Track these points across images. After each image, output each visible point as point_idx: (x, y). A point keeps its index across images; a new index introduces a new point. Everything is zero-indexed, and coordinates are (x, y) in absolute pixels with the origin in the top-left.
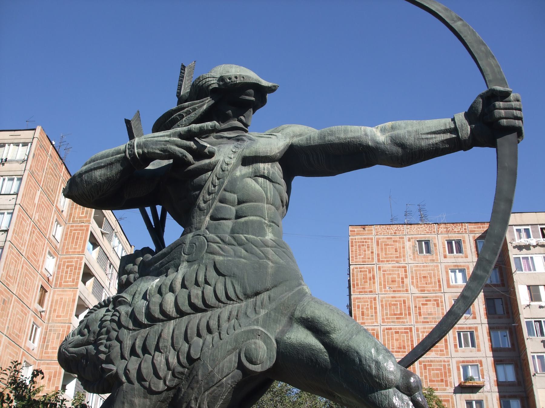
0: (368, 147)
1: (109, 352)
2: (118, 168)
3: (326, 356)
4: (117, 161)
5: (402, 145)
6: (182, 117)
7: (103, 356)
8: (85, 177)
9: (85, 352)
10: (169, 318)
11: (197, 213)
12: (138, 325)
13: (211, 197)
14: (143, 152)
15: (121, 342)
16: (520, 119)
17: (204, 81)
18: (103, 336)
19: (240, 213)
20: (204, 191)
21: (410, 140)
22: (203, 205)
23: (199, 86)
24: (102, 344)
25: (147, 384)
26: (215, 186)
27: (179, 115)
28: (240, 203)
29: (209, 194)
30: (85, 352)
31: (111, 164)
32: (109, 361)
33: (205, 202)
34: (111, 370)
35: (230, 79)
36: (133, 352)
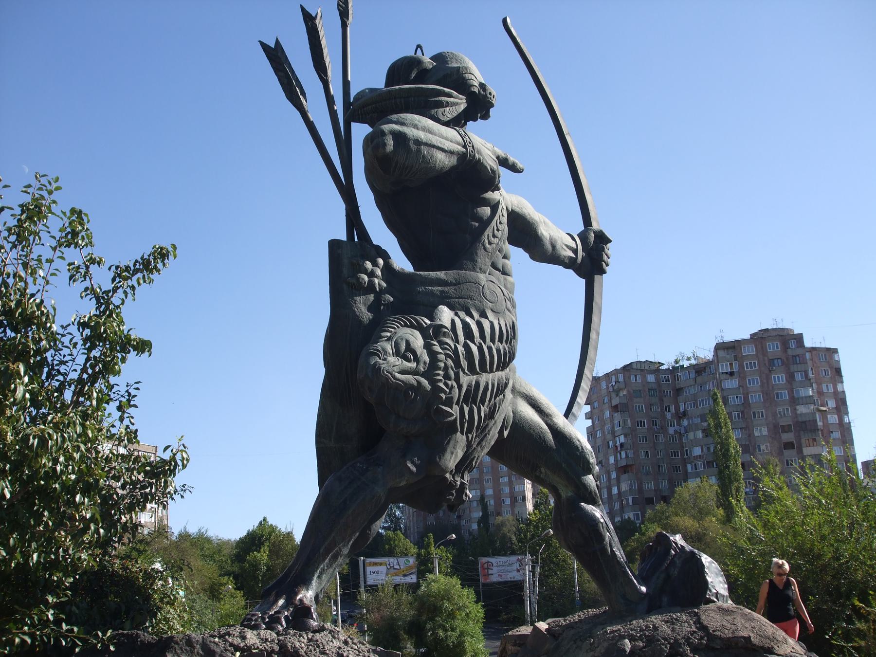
0: (537, 234)
1: (450, 393)
2: (452, 161)
3: (549, 436)
4: (458, 153)
5: (554, 246)
6: (448, 104)
7: (443, 396)
8: (425, 150)
9: (415, 383)
10: (491, 371)
11: (481, 252)
12: (472, 370)
13: (496, 241)
14: (479, 159)
15: (460, 387)
16: (607, 265)
17: (471, 76)
18: (440, 372)
19: (507, 270)
20: (489, 231)
21: (559, 245)
22: (488, 246)
23: (464, 78)
24: (440, 381)
25: (470, 436)
26: (498, 230)
27: (447, 102)
28: (505, 257)
29: (494, 236)
30: (415, 383)
31: (451, 153)
32: (449, 402)
33: (490, 243)
34: (451, 415)
35: (490, 94)
36: (465, 401)
